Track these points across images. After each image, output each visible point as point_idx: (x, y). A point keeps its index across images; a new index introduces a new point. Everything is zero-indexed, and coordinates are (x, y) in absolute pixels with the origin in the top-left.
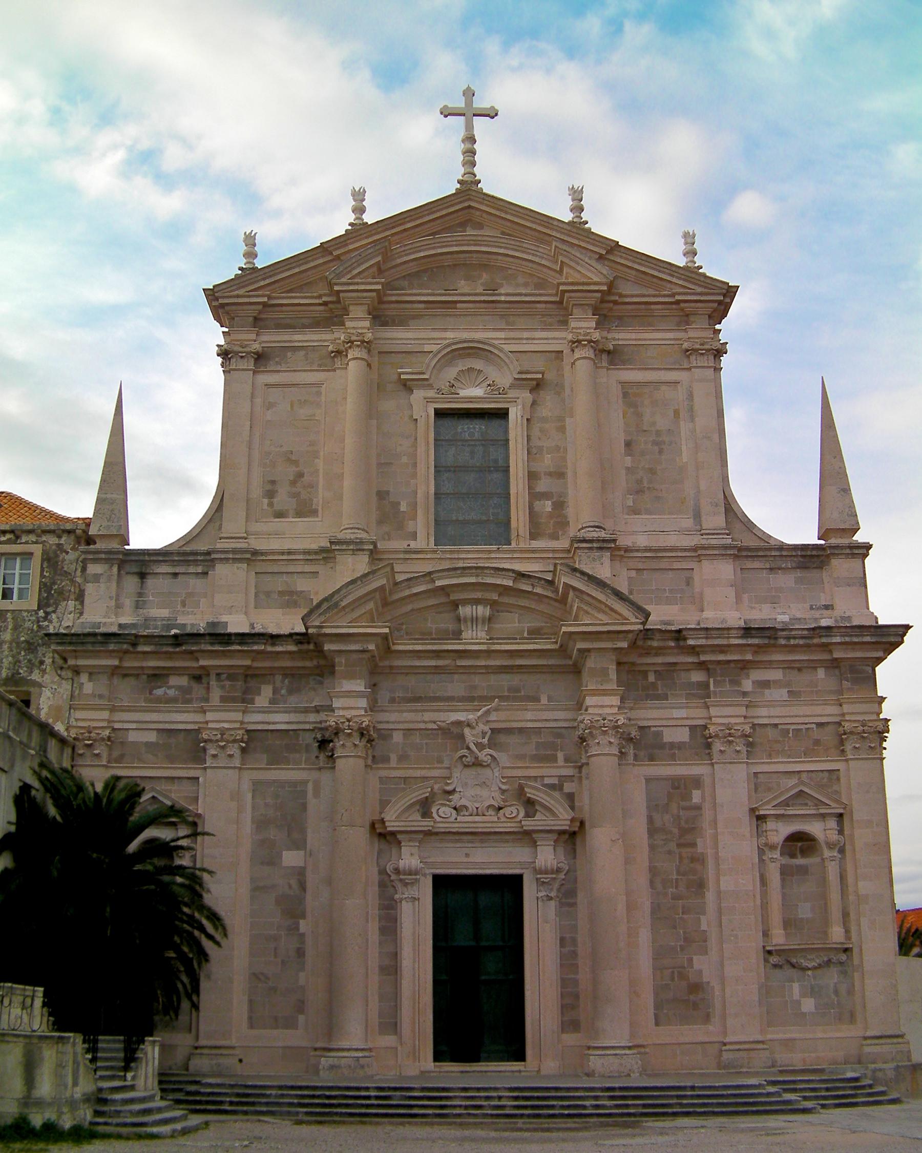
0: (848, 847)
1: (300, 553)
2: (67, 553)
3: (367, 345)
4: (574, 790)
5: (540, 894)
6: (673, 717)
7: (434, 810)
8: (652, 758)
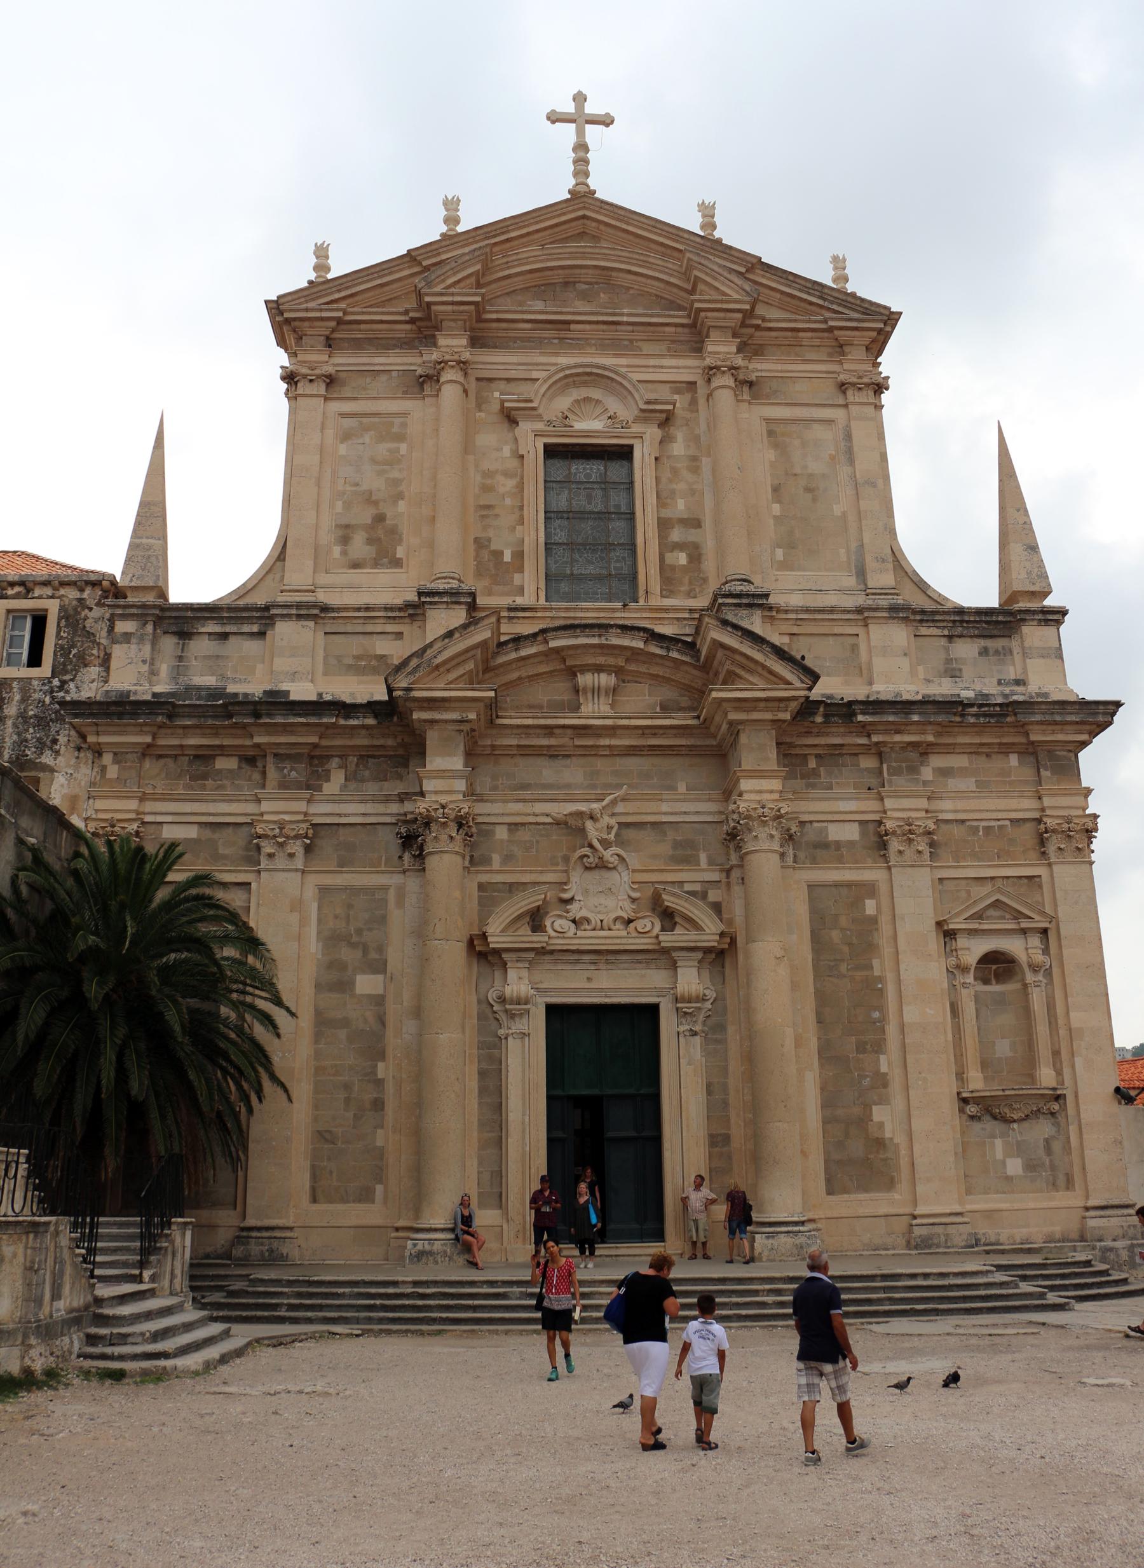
0: (1056, 971)
1: (379, 609)
2: (91, 609)
3: (463, 365)
4: (720, 899)
5: (682, 1029)
6: (839, 809)
7: (548, 923)
8: (814, 860)
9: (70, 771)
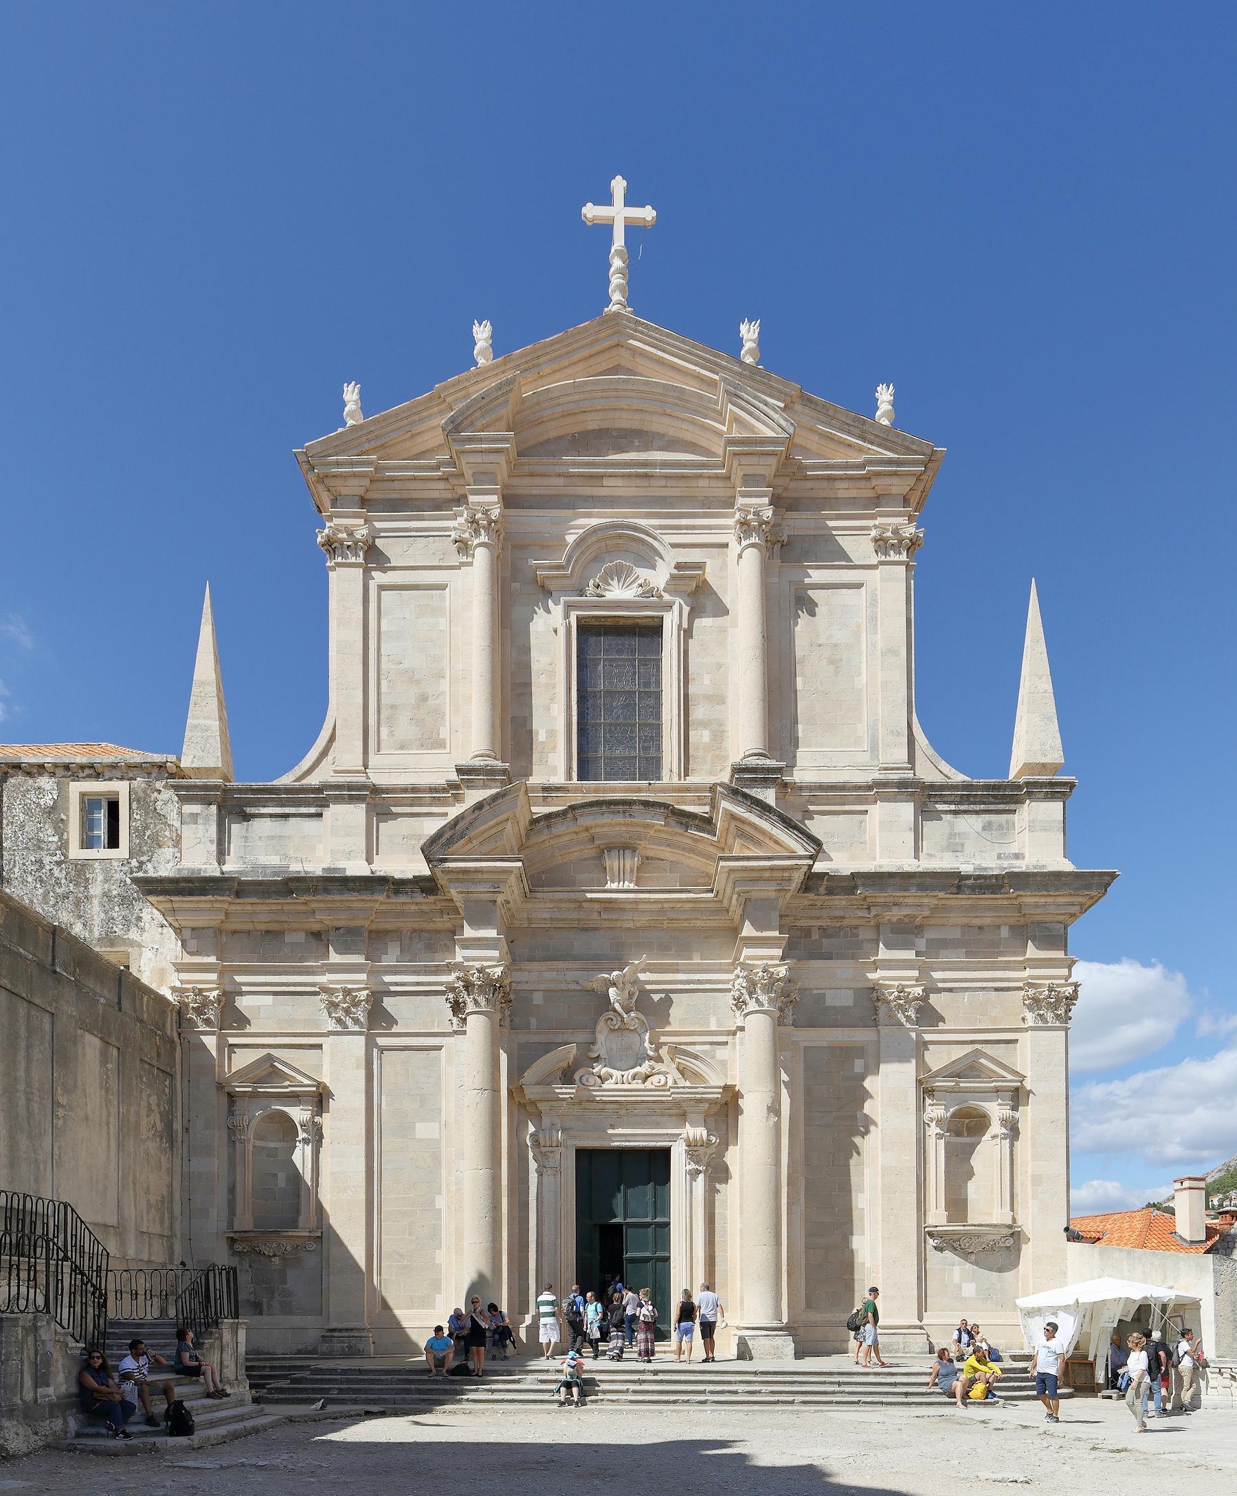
1: (424, 791)
2: (159, 792)
9: (156, 947)
